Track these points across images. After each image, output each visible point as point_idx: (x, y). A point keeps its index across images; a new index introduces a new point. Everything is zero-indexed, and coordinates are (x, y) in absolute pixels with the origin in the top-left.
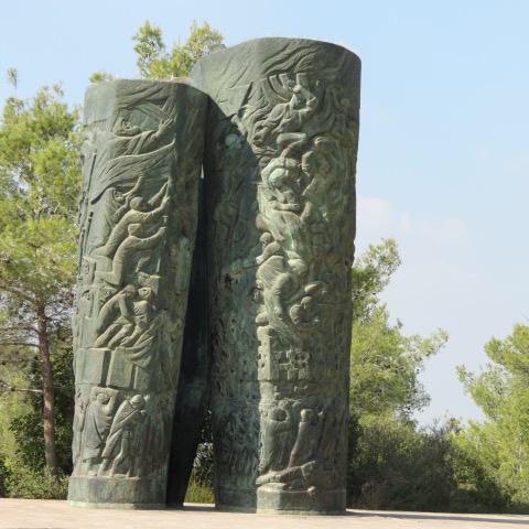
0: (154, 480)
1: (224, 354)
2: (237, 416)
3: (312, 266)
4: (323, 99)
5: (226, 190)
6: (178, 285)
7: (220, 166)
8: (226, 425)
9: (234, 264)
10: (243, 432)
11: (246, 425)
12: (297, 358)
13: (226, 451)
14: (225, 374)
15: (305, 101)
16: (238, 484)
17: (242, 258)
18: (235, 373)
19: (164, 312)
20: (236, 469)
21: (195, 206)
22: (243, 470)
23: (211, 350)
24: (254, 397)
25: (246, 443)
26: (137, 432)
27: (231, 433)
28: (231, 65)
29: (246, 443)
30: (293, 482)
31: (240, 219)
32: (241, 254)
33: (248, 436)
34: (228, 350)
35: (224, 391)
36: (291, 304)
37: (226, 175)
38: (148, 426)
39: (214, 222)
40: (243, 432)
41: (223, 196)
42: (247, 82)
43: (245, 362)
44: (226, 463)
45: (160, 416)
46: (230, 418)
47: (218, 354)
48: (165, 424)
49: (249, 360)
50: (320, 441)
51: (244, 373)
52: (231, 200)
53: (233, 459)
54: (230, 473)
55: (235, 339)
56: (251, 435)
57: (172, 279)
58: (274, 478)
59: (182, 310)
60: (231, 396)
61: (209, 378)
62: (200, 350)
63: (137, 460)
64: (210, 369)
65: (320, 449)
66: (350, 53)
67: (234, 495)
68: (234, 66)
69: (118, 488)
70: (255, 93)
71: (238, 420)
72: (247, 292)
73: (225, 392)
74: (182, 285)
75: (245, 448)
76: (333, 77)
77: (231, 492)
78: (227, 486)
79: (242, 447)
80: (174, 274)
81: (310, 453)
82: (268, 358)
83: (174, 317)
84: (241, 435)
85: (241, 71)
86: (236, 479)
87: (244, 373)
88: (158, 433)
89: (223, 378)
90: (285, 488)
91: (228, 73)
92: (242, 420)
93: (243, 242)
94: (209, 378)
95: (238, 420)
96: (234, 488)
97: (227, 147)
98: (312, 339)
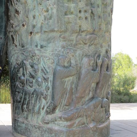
1: (17, 12)
2: (27, 63)
8: (18, 71)
10: (33, 77)
11: (35, 71)
13: (19, 92)
14: (17, 28)
16: (29, 119)
18: (26, 27)
20: (27, 108)
24: (42, 47)
25: (35, 86)
27: (23, 78)
29: (35, 86)
30: (77, 121)
33: (37, 81)
34: (20, 8)
35: (16, 42)
40: (33, 77)
43: (34, 17)
44: (20, 102)
46: (22, 65)
47: (12, 13)
49: (37, 14)
50: (97, 84)
51: (34, 27)
53: (25, 99)
54: (23, 110)
56: (40, 80)
58: (60, 118)
60: (23, 47)
61: (5, 34)
64: (6, 27)
65: (98, 91)
67: (26, 129)
71: (29, 66)
73: (18, 44)
75: (35, 91)
77: (24, 125)
78: (20, 120)
79: (31, 90)
81: (91, 95)
82: (55, 11)
84: (31, 79)
86: (27, 115)
87: (34, 27)
89: (16, 32)
90: (71, 126)
92: (32, 67)
94: (5, 34)
95: (29, 66)
96: (26, 122)
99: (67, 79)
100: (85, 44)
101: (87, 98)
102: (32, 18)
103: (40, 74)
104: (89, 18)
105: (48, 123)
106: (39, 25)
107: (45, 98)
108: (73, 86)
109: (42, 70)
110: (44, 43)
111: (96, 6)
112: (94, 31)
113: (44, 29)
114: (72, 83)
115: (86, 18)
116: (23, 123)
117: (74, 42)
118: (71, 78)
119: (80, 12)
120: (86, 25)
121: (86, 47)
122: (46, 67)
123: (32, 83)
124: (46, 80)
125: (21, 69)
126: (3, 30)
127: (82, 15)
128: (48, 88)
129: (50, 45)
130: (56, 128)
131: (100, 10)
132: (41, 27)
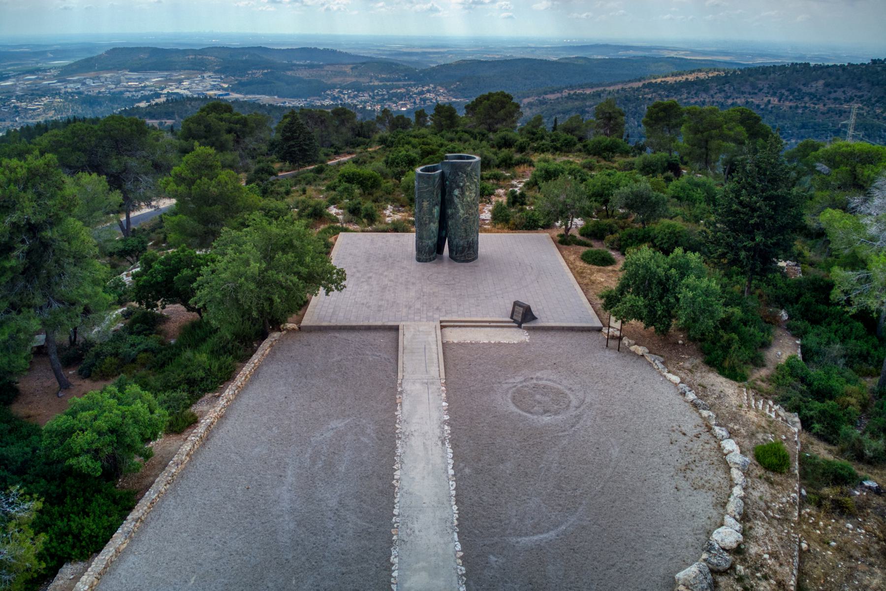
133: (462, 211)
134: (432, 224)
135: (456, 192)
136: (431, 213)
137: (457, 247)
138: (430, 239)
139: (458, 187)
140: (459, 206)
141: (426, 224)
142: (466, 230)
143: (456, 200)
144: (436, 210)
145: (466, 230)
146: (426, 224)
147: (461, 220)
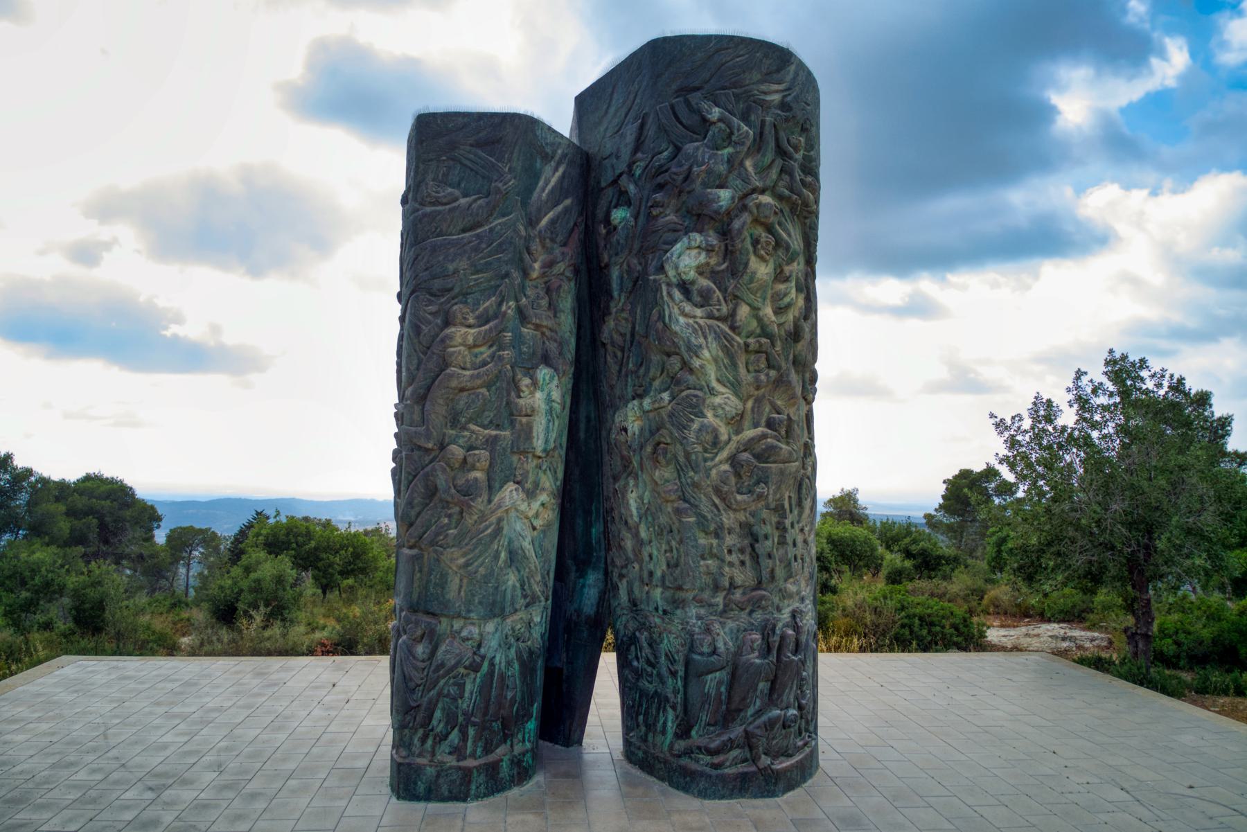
0: (506, 758)
2: (643, 637)
3: (750, 404)
4: (761, 134)
5: (616, 294)
6: (539, 444)
7: (606, 258)
9: (630, 405)
12: (730, 552)
15: (732, 133)
17: (640, 397)
19: (511, 486)
20: (645, 721)
21: (567, 322)
22: (655, 725)
23: (606, 532)
24: (665, 612)
26: (468, 687)
27: (635, 663)
28: (615, 96)
31: (637, 337)
32: (640, 391)
33: (659, 674)
36: (715, 466)
37: (615, 273)
38: (491, 673)
39: (604, 345)
41: (612, 304)
42: (635, 119)
43: (651, 556)
45: (513, 651)
48: (523, 664)
52: (623, 310)
53: (640, 705)
55: (636, 519)
57: (528, 432)
59: (549, 482)
62: (594, 530)
63: (471, 732)
66: (801, 66)
68: (618, 99)
69: (441, 781)
70: (651, 130)
71: (645, 645)
72: (649, 449)
74: (547, 441)
75: (656, 692)
76: (776, 98)
80: (529, 428)
83: (530, 495)
84: (649, 669)
85: (629, 102)
86: (646, 735)
88: (510, 683)
91: (612, 110)
92: (650, 645)
93: (642, 371)
97: (615, 228)
98: (752, 520)
99: (710, 676)
100: (742, 609)
101: (750, 711)
102: (647, 559)
103: (663, 659)
104: (748, 563)
105: (679, 756)
106: (659, 573)
107: (674, 708)
108: (723, 689)
109: (666, 655)
110: (668, 608)
111: (761, 538)
112: (760, 583)
113: (667, 583)
114: (720, 683)
115: (743, 563)
116: (639, 748)
117: (721, 607)
118: (718, 674)
119: (730, 552)
120: (743, 577)
121: (744, 615)
122: (673, 650)
123: (651, 676)
124: (674, 674)
125: (633, 648)
126: (603, 565)
127: (733, 558)
128: (676, 692)
129: (679, 612)
130: (693, 766)
131: (768, 543)
132: (663, 577)
133: (725, 399)
134: (510, 494)
135: (688, 258)
136: (510, 415)
137: (692, 673)
138: (496, 609)
139: (699, 217)
140: (708, 358)
141: (468, 492)
142: (751, 536)
143: (683, 318)
144: (545, 397)
145: (751, 536)
146: (468, 492)
147: (720, 466)
